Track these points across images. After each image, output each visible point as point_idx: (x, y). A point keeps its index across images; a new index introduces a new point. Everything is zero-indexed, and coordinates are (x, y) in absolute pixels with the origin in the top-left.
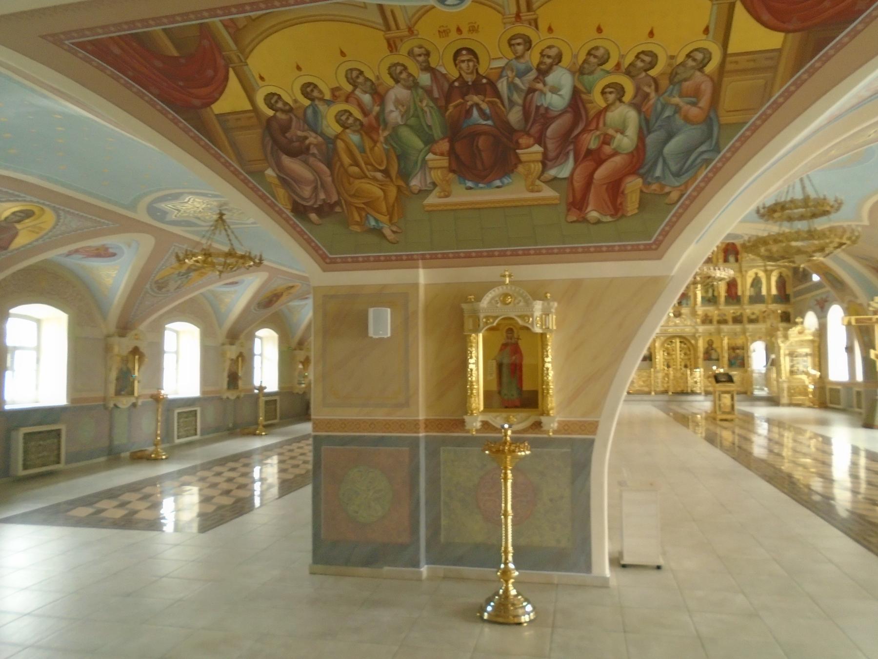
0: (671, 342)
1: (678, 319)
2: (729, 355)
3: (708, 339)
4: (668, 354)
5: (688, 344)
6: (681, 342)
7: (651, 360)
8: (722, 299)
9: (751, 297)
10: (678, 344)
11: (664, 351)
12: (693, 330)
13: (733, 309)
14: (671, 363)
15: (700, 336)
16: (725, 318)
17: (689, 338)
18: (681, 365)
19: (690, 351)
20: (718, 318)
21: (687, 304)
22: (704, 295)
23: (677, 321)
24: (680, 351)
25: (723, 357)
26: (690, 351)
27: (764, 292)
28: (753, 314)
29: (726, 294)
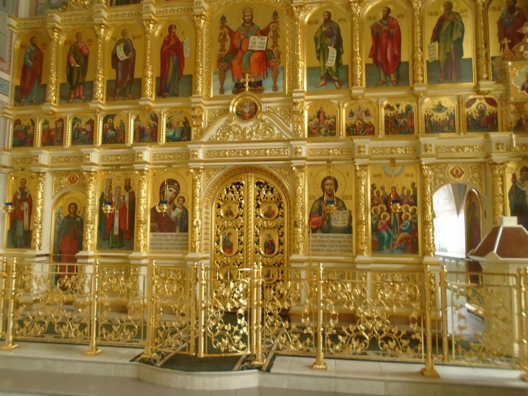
0: (239, 184)
1: (251, 123)
2: (376, 218)
3: (324, 175)
4: (229, 213)
5: (277, 188)
6: (258, 184)
7: (185, 229)
8: (360, 72)
9: (432, 66)
10: (253, 188)
11: (219, 206)
12: (288, 153)
13: (390, 98)
14: (234, 239)
15: (300, 168)
16: (366, 120)
17: (275, 173)
18: (257, 242)
19: (280, 207)
20: (353, 120)
21: (275, 88)
22: (316, 63)
23: (249, 125)
24: (258, 206)
25: (359, 223)
26: (280, 207)
27: (468, 52)
28: (440, 108)
29: (371, 61)
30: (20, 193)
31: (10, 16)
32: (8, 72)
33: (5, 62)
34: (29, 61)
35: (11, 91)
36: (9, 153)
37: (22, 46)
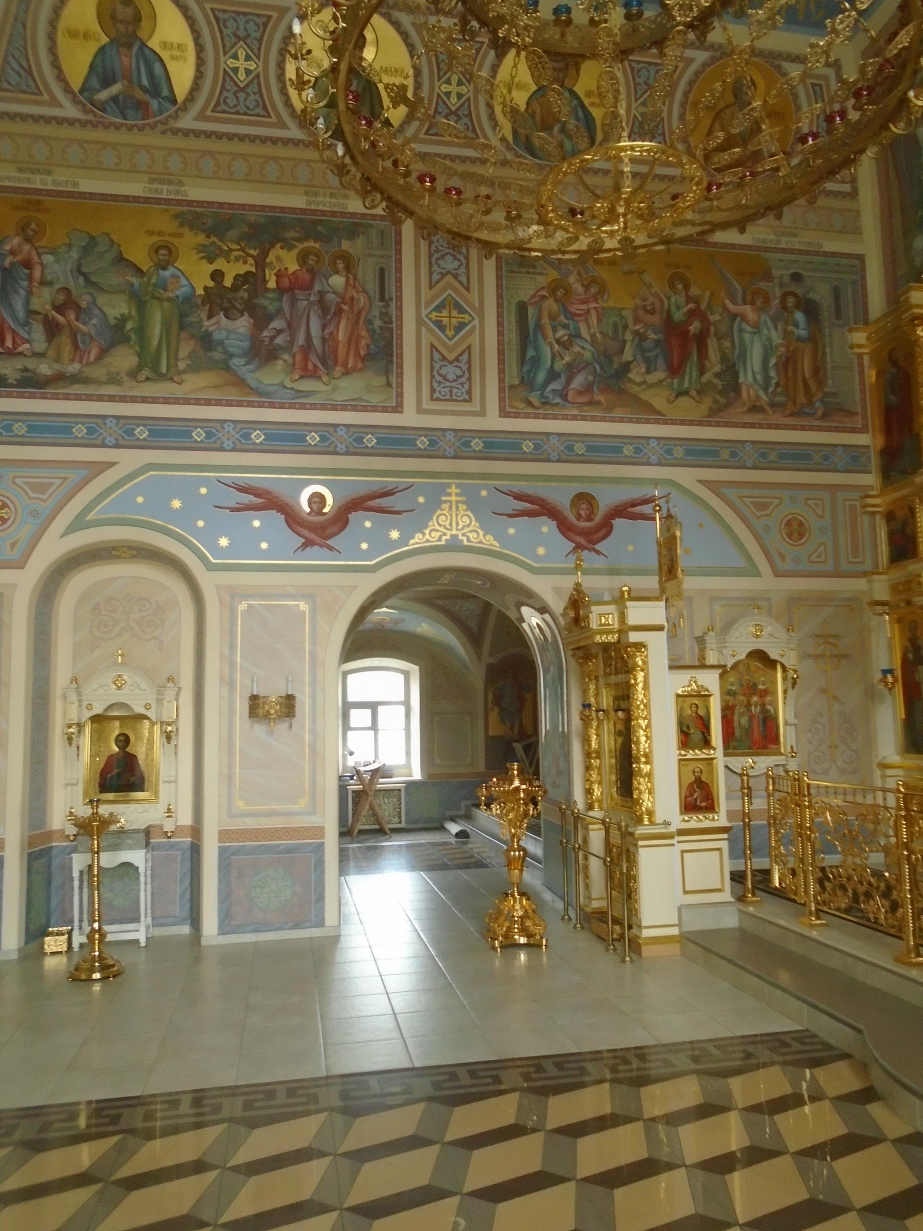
30: (911, 649)
31: (851, 330)
32: (863, 430)
33: (857, 414)
34: (892, 397)
35: (875, 462)
36: (884, 577)
37: (879, 375)
